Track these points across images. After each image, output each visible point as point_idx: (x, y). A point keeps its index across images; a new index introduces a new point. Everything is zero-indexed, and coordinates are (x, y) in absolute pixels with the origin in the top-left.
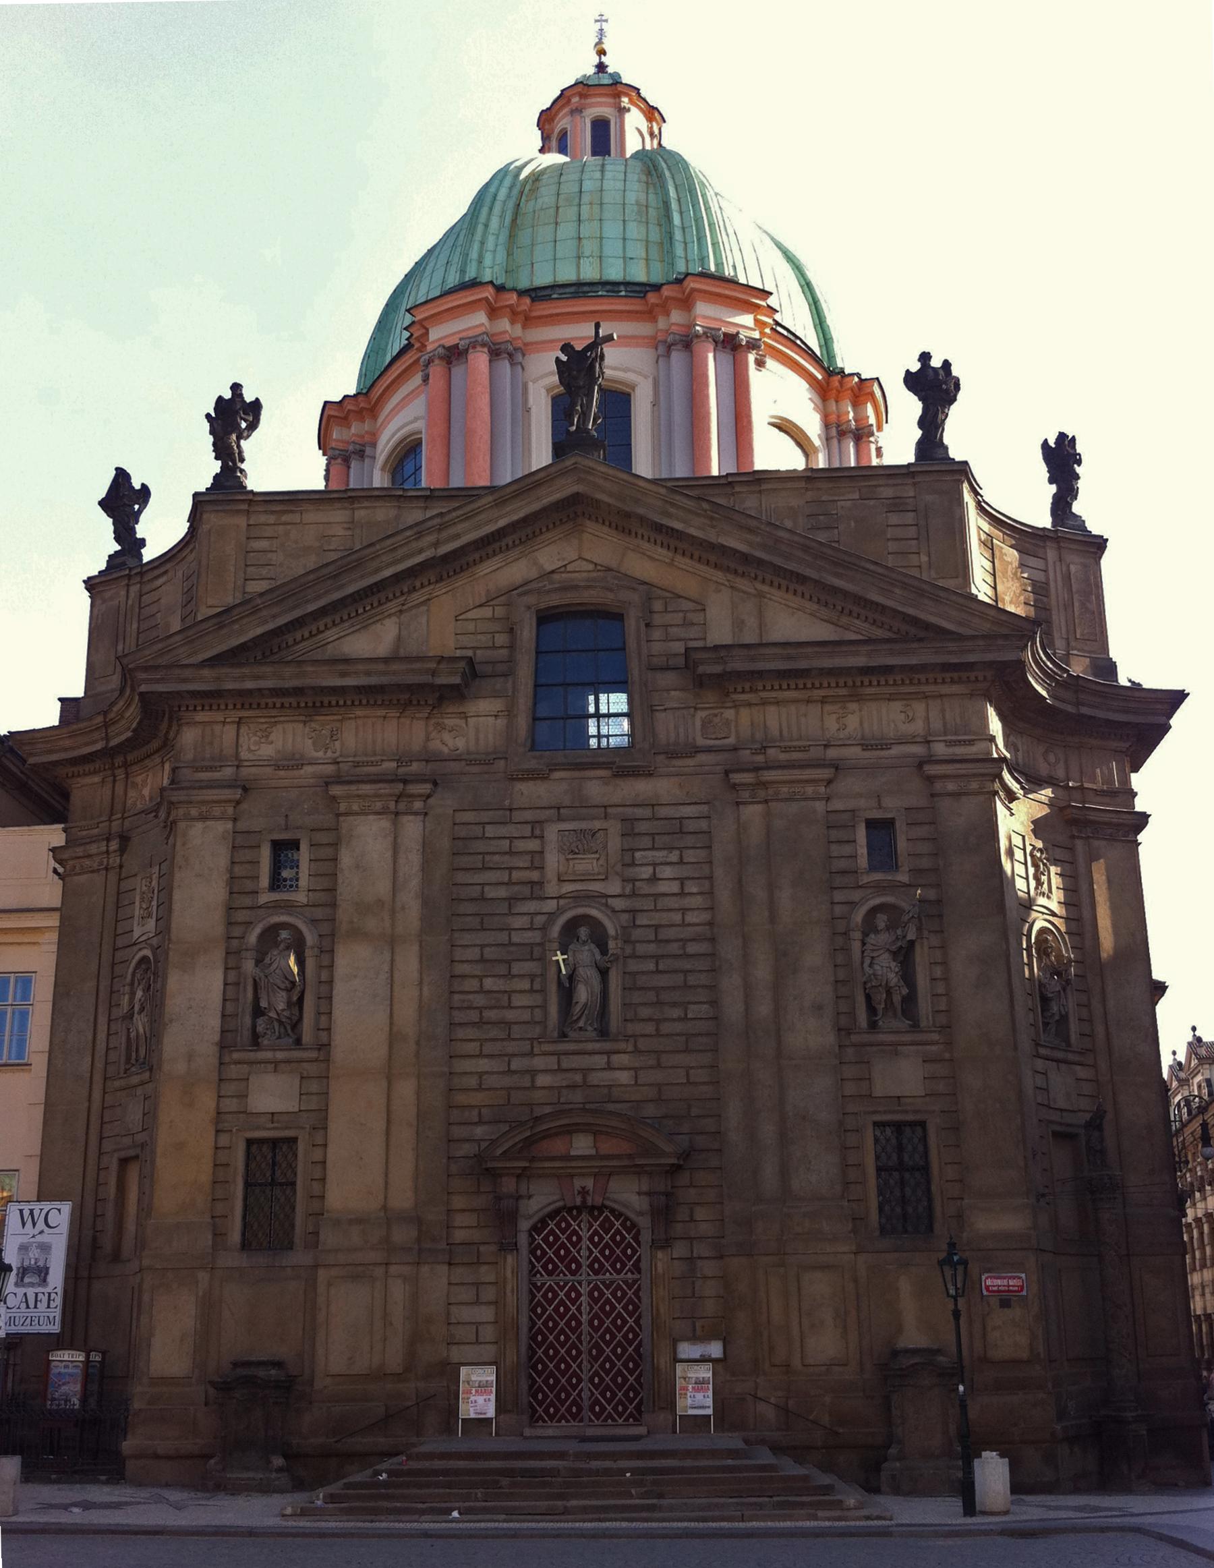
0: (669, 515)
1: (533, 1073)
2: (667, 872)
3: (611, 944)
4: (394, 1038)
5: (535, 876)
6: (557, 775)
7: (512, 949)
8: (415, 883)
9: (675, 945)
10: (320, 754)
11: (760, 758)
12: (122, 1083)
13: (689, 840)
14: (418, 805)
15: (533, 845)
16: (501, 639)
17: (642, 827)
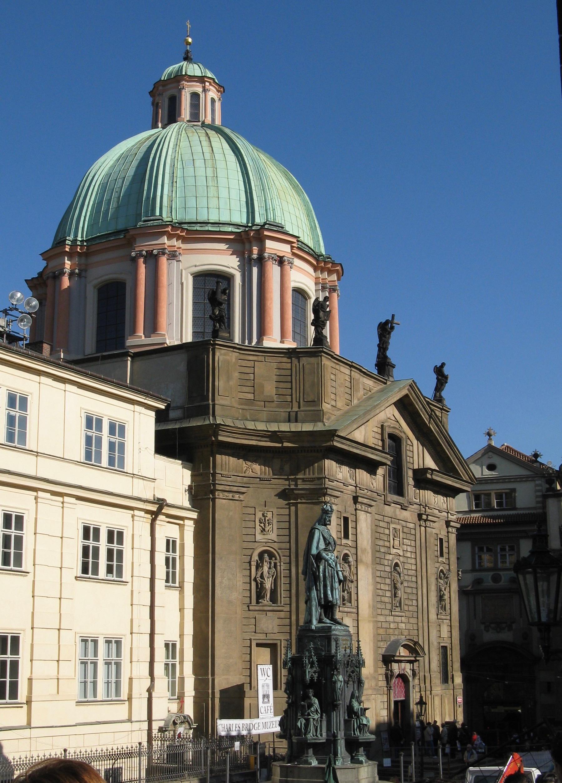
0: (422, 411)
1: (390, 623)
2: (409, 549)
3: (402, 575)
4: (369, 606)
5: (387, 544)
6: (393, 505)
7: (385, 573)
8: (370, 541)
9: (410, 577)
10: (350, 481)
11: (424, 509)
12: (257, 608)
13: (412, 537)
14: (369, 510)
15: (387, 531)
16: (380, 443)
17: (406, 530)
